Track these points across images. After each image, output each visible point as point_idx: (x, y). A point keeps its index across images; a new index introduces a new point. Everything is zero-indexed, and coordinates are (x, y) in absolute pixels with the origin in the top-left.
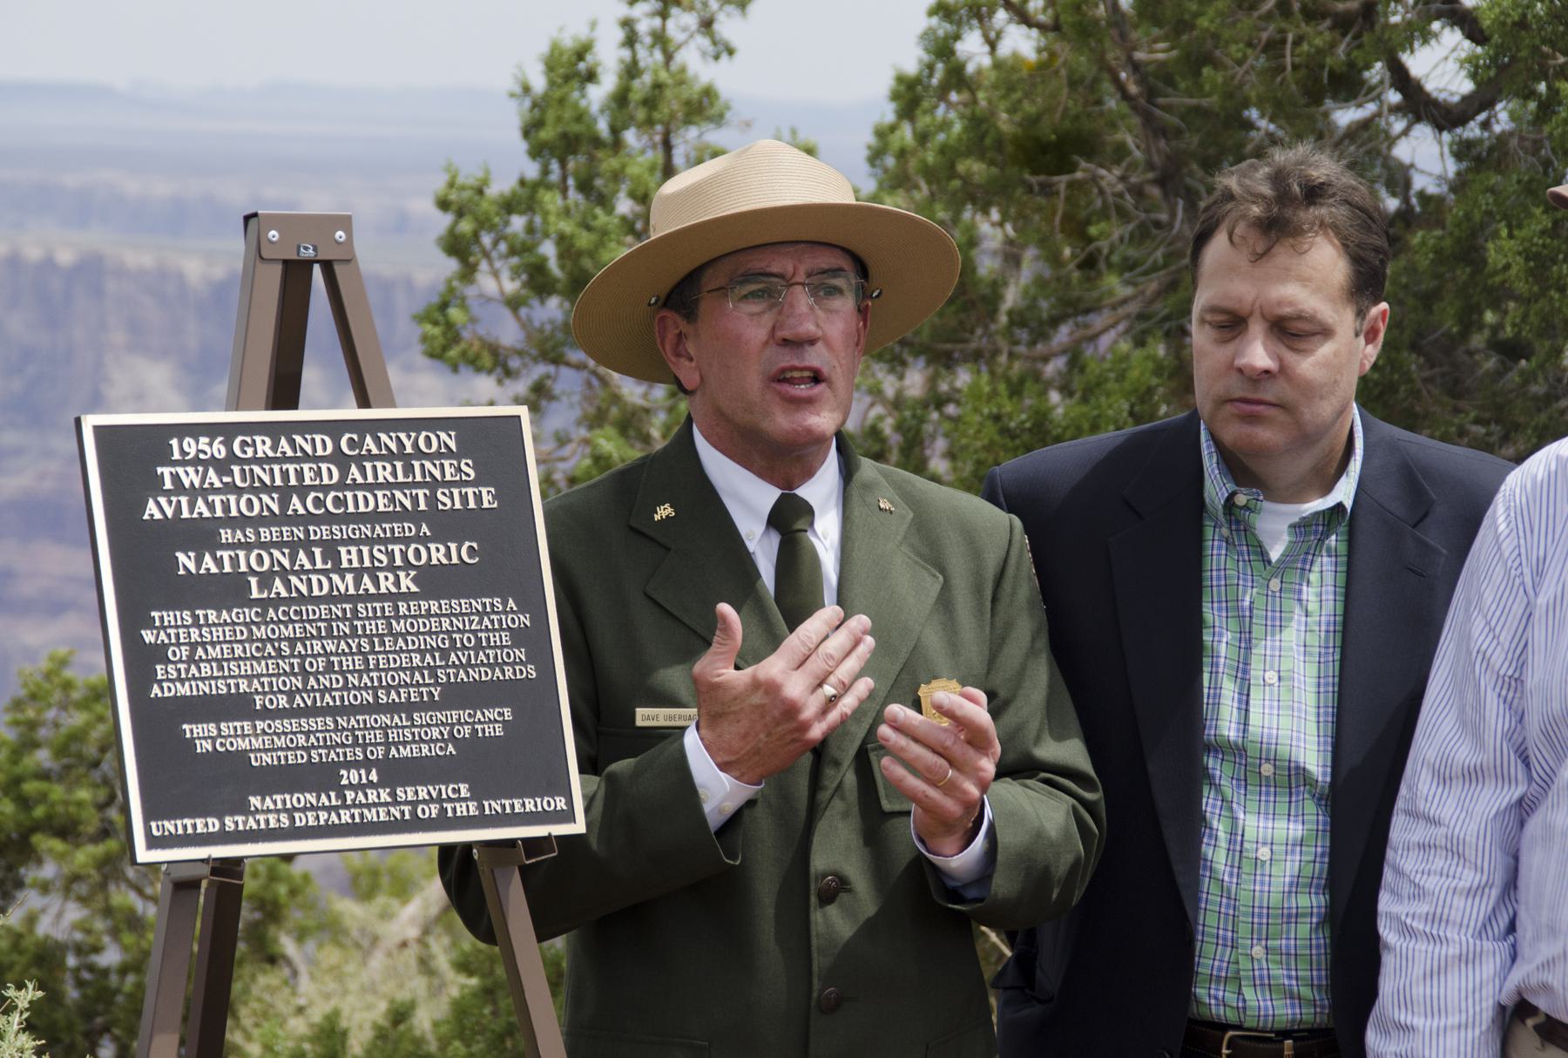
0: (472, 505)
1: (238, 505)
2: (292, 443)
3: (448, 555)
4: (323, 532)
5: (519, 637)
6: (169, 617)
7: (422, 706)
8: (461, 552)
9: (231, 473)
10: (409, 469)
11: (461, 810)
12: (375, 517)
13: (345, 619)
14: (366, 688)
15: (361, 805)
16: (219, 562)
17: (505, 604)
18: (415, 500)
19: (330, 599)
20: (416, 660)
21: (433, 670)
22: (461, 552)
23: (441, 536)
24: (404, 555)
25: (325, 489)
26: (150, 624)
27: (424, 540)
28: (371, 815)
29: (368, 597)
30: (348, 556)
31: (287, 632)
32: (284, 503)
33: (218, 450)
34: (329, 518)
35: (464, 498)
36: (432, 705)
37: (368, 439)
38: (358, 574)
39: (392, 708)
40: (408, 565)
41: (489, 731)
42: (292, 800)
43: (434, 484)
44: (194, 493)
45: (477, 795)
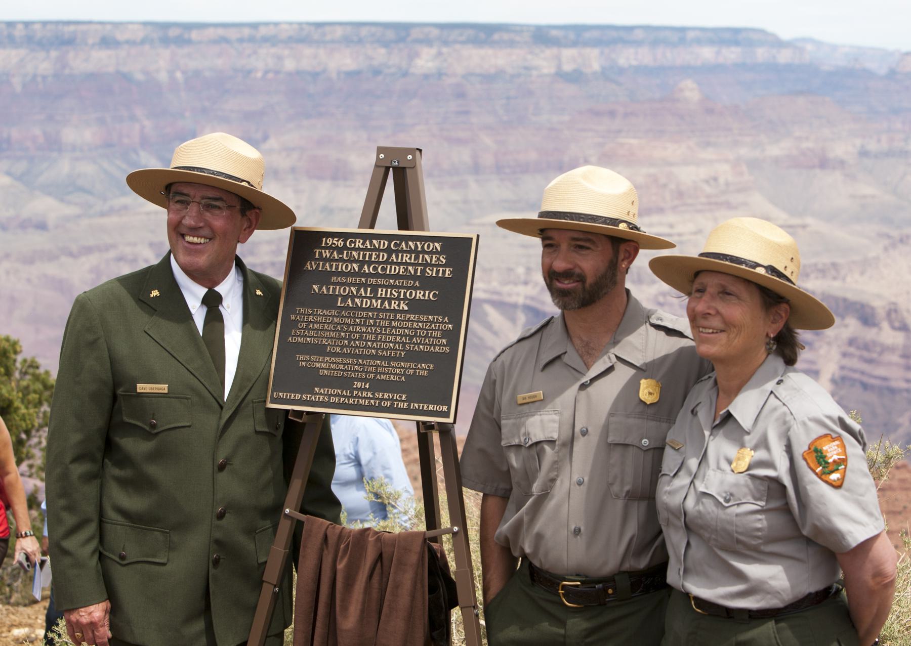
0: (440, 275)
1: (342, 267)
2: (371, 243)
3: (424, 295)
4: (373, 281)
5: (445, 334)
6: (302, 310)
7: (395, 359)
8: (430, 295)
9: (343, 254)
10: (417, 258)
11: (401, 405)
12: (397, 276)
13: (372, 318)
14: (374, 348)
15: (359, 397)
16: (328, 289)
17: (443, 319)
18: (416, 271)
19: (368, 309)
20: (398, 339)
21: (404, 344)
22: (430, 295)
23: (423, 288)
24: (405, 293)
25: (380, 263)
26: (294, 313)
27: (416, 289)
28: (362, 402)
29: (385, 310)
30: (381, 292)
31: (348, 321)
32: (361, 268)
33: (340, 243)
34: (377, 275)
35: (438, 272)
36: (399, 359)
37: (403, 244)
38: (383, 300)
39: (382, 358)
40: (405, 299)
41: (422, 373)
42: (331, 391)
43: (427, 265)
44: (326, 260)
45: (409, 400)
